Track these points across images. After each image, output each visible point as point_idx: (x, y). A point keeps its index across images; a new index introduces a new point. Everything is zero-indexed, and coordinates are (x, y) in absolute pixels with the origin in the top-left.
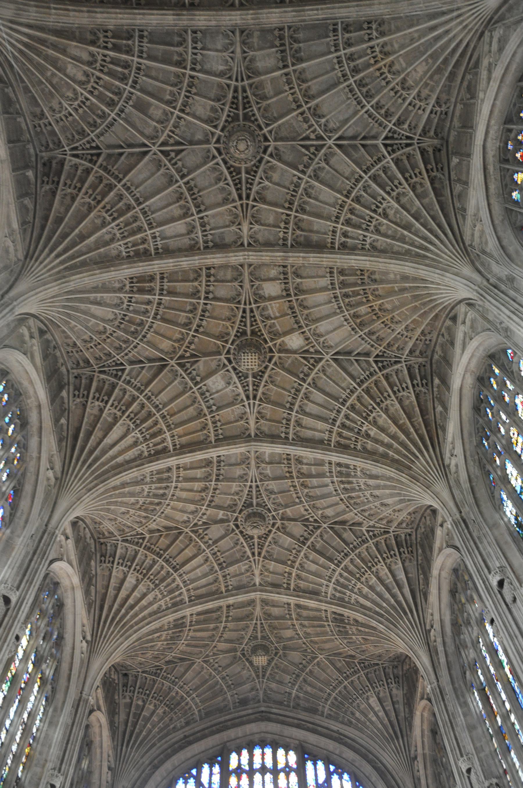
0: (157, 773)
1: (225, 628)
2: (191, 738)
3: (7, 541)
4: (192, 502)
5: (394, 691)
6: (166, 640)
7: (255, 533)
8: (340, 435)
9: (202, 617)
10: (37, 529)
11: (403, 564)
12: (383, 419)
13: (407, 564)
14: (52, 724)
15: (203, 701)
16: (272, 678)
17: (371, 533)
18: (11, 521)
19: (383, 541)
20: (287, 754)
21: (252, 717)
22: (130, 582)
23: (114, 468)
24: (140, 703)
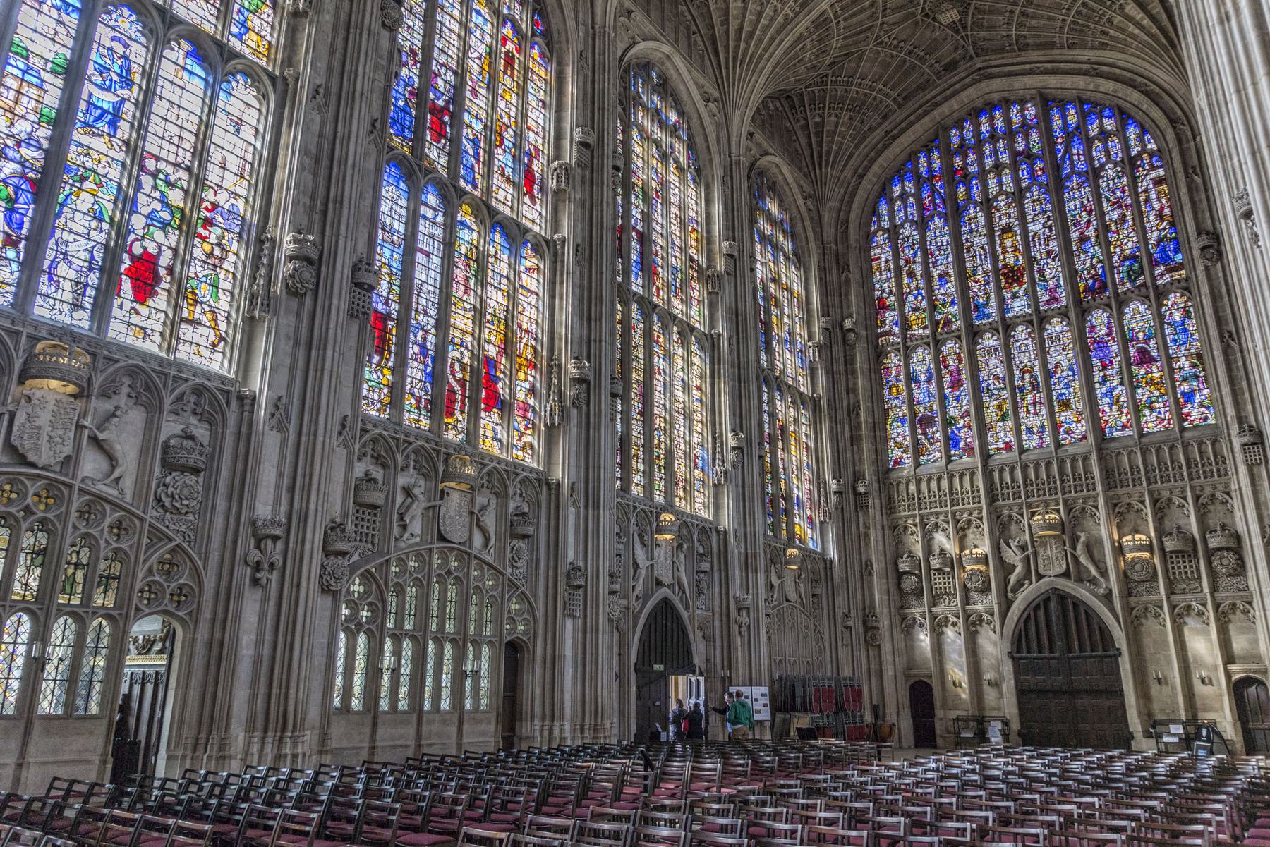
0: (864, 182)
16: (977, 25)
20: (1023, 110)
24: (817, 119)
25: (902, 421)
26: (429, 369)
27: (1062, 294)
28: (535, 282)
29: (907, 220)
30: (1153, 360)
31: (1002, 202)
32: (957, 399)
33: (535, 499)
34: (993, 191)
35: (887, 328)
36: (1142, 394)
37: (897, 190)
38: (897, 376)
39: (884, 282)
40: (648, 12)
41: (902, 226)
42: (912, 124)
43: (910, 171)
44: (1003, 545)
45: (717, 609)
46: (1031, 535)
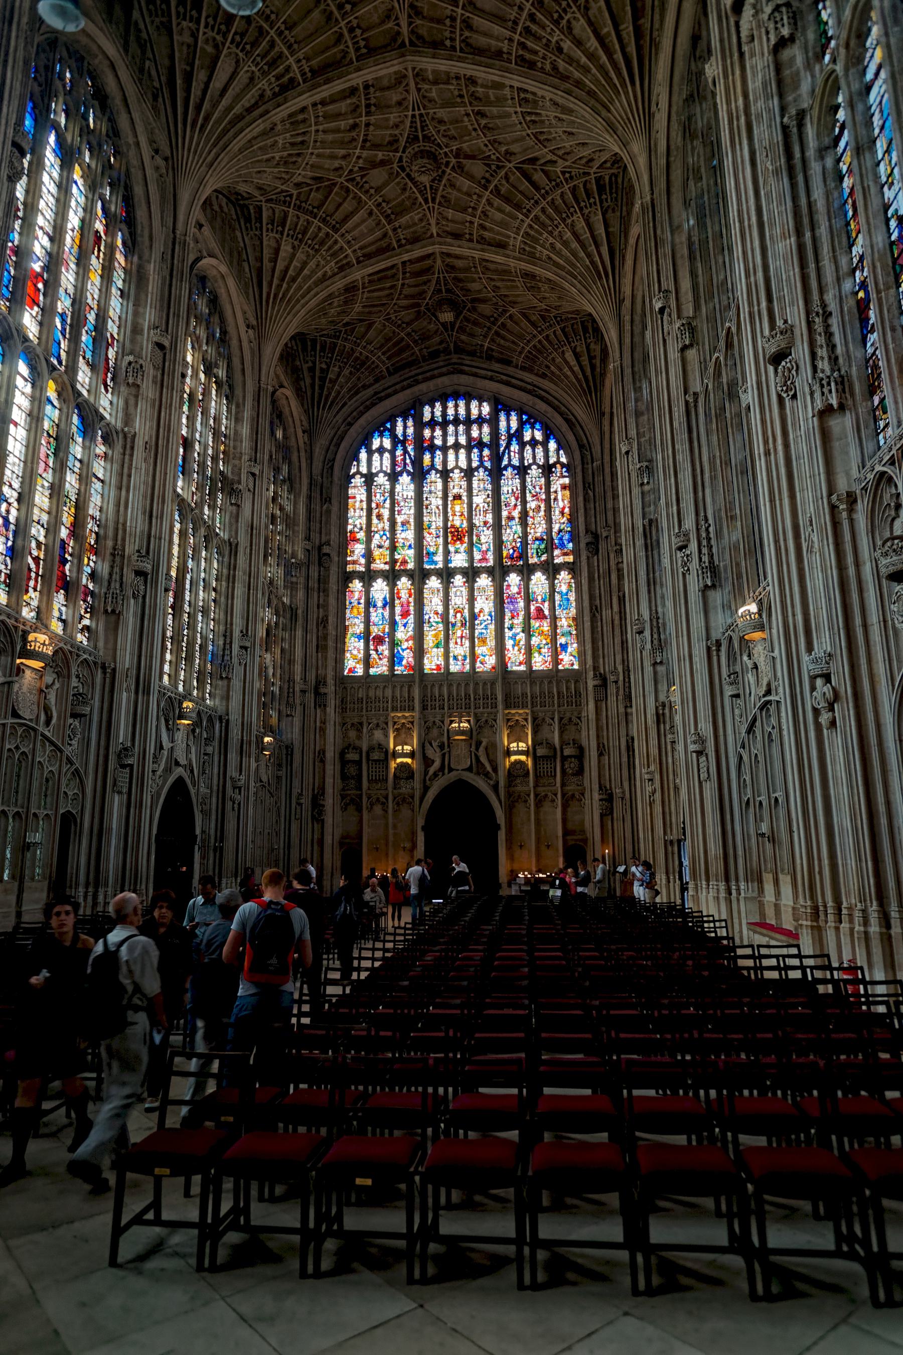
1: (403, 285)
2: (383, 394)
3: (138, 271)
4: (342, 144)
5: (592, 346)
6: (339, 306)
7: (425, 179)
8: (523, 46)
9: (375, 277)
10: (165, 244)
11: (604, 215)
12: (580, 26)
13: (610, 214)
14: (238, 420)
15: (389, 358)
16: (462, 329)
17: (567, 175)
18: (134, 243)
19: (581, 186)
20: (480, 406)
21: (444, 370)
22: (286, 251)
23: (233, 123)
24: (324, 366)
25: (359, 637)
26: (10, 543)
27: (490, 556)
28: (102, 470)
29: (381, 471)
31: (456, 475)
32: (405, 626)
33: (90, 682)
34: (451, 464)
35: (355, 558)
36: (535, 641)
37: (376, 443)
38: (359, 599)
39: (356, 519)
40: (213, 228)
41: (376, 475)
42: (396, 392)
43: (389, 430)
44: (427, 745)
45: (215, 788)
46: (449, 738)
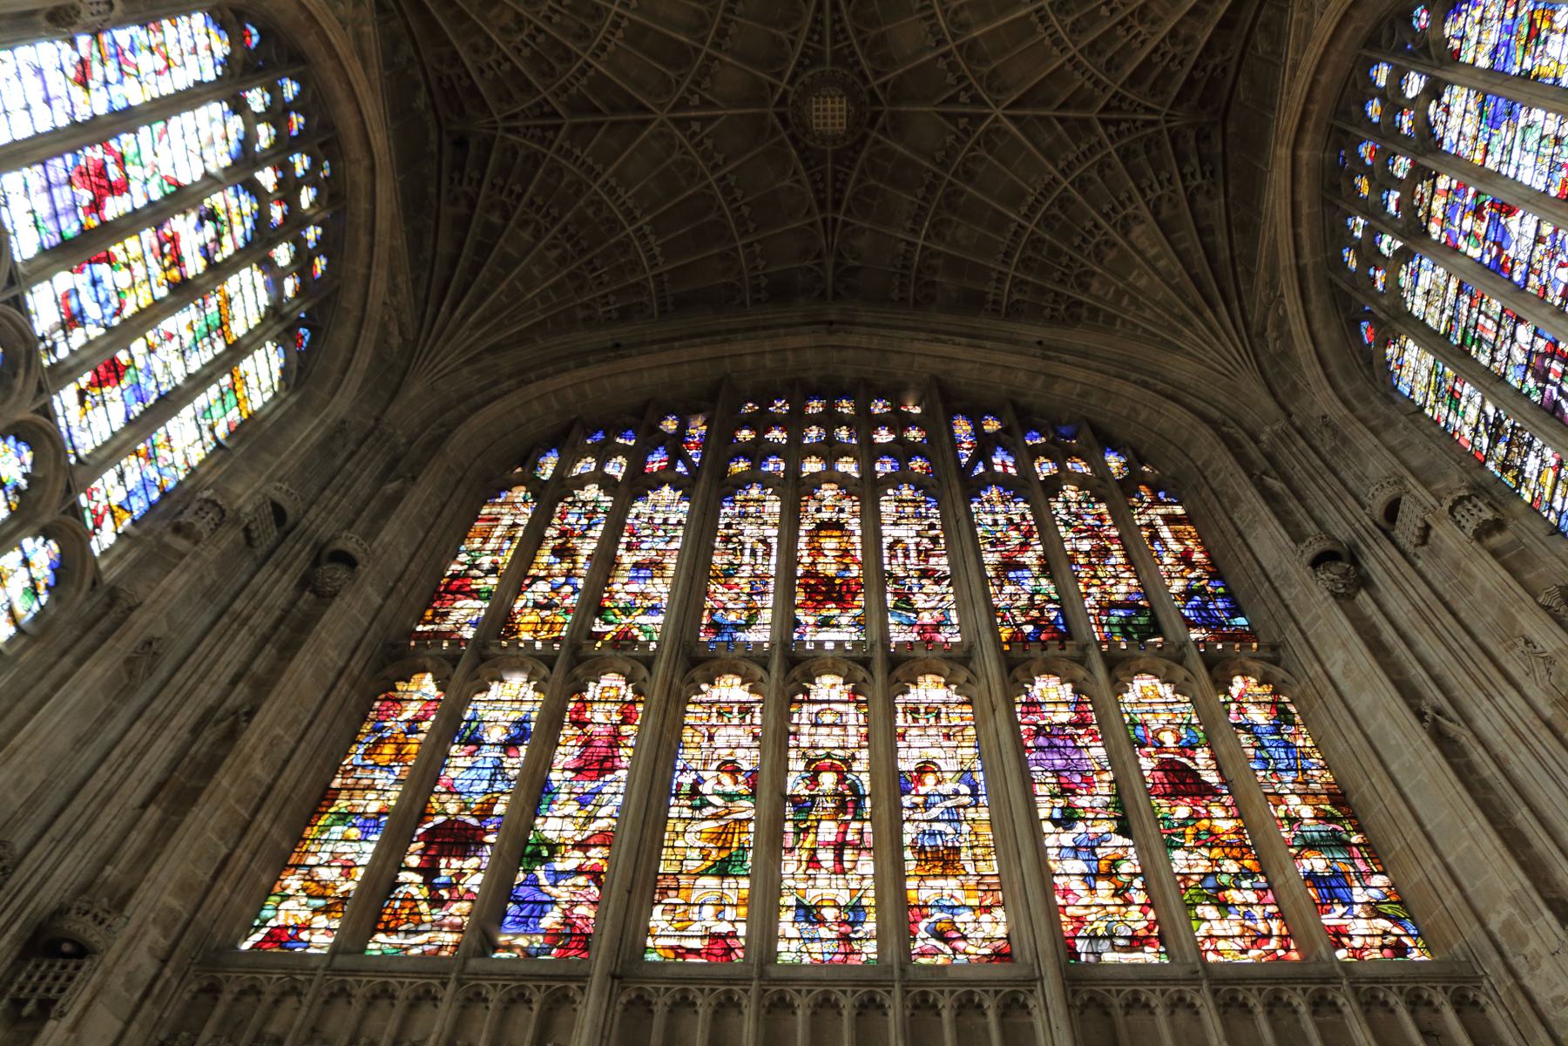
24: (496, 218)
30: (1206, 791)
